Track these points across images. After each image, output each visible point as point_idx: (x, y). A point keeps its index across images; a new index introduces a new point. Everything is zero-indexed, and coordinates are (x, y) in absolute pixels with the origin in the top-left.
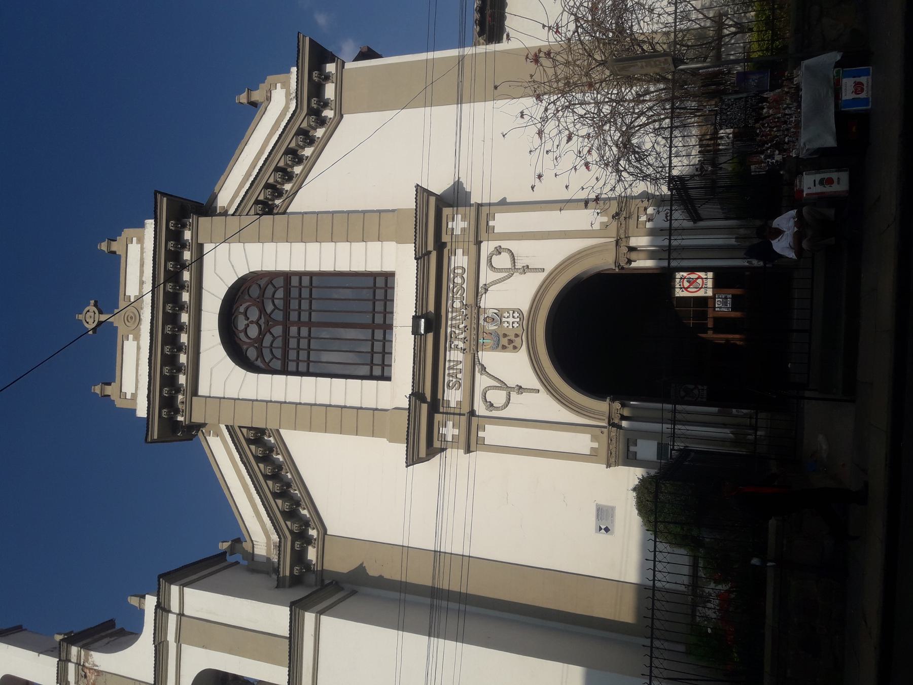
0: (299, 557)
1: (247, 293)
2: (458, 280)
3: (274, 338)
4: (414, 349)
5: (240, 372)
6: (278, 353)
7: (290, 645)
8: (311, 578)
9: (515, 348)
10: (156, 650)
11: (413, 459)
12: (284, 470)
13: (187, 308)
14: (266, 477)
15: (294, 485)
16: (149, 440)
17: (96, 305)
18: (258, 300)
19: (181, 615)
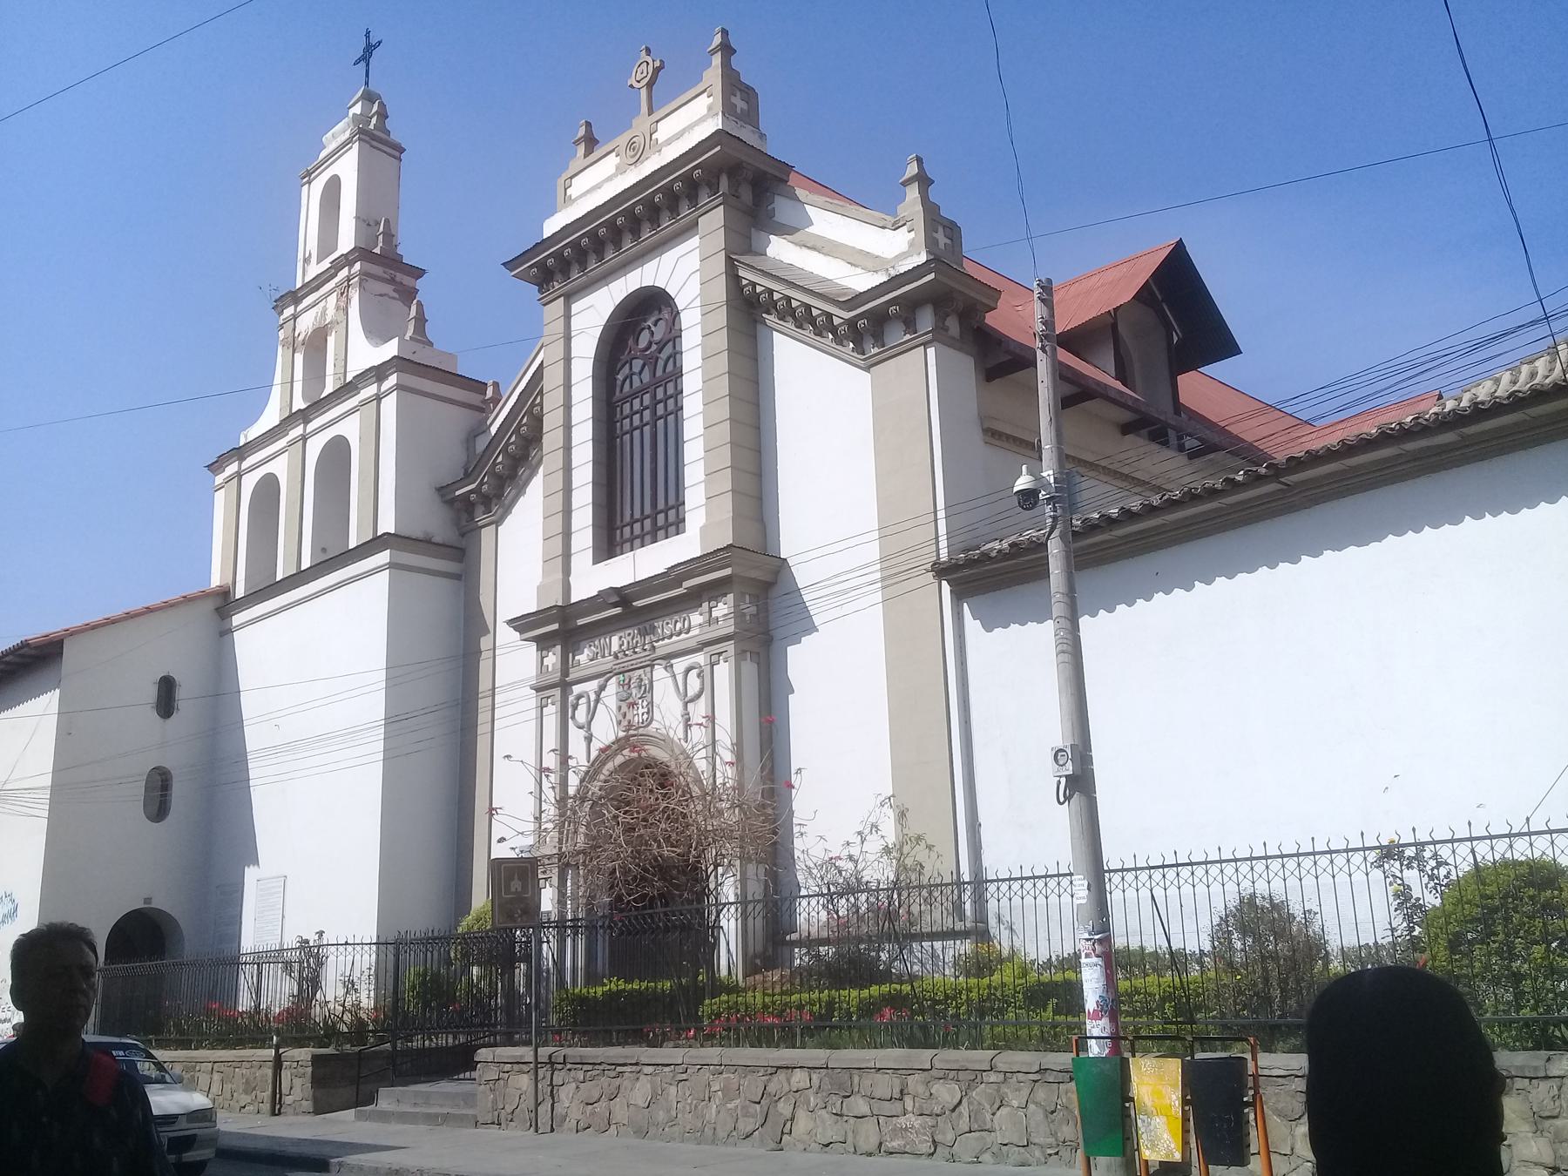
2: (679, 625)
8: (465, 516)
9: (619, 723)
11: (522, 624)
17: (657, 71)
18: (673, 331)
19: (378, 398)
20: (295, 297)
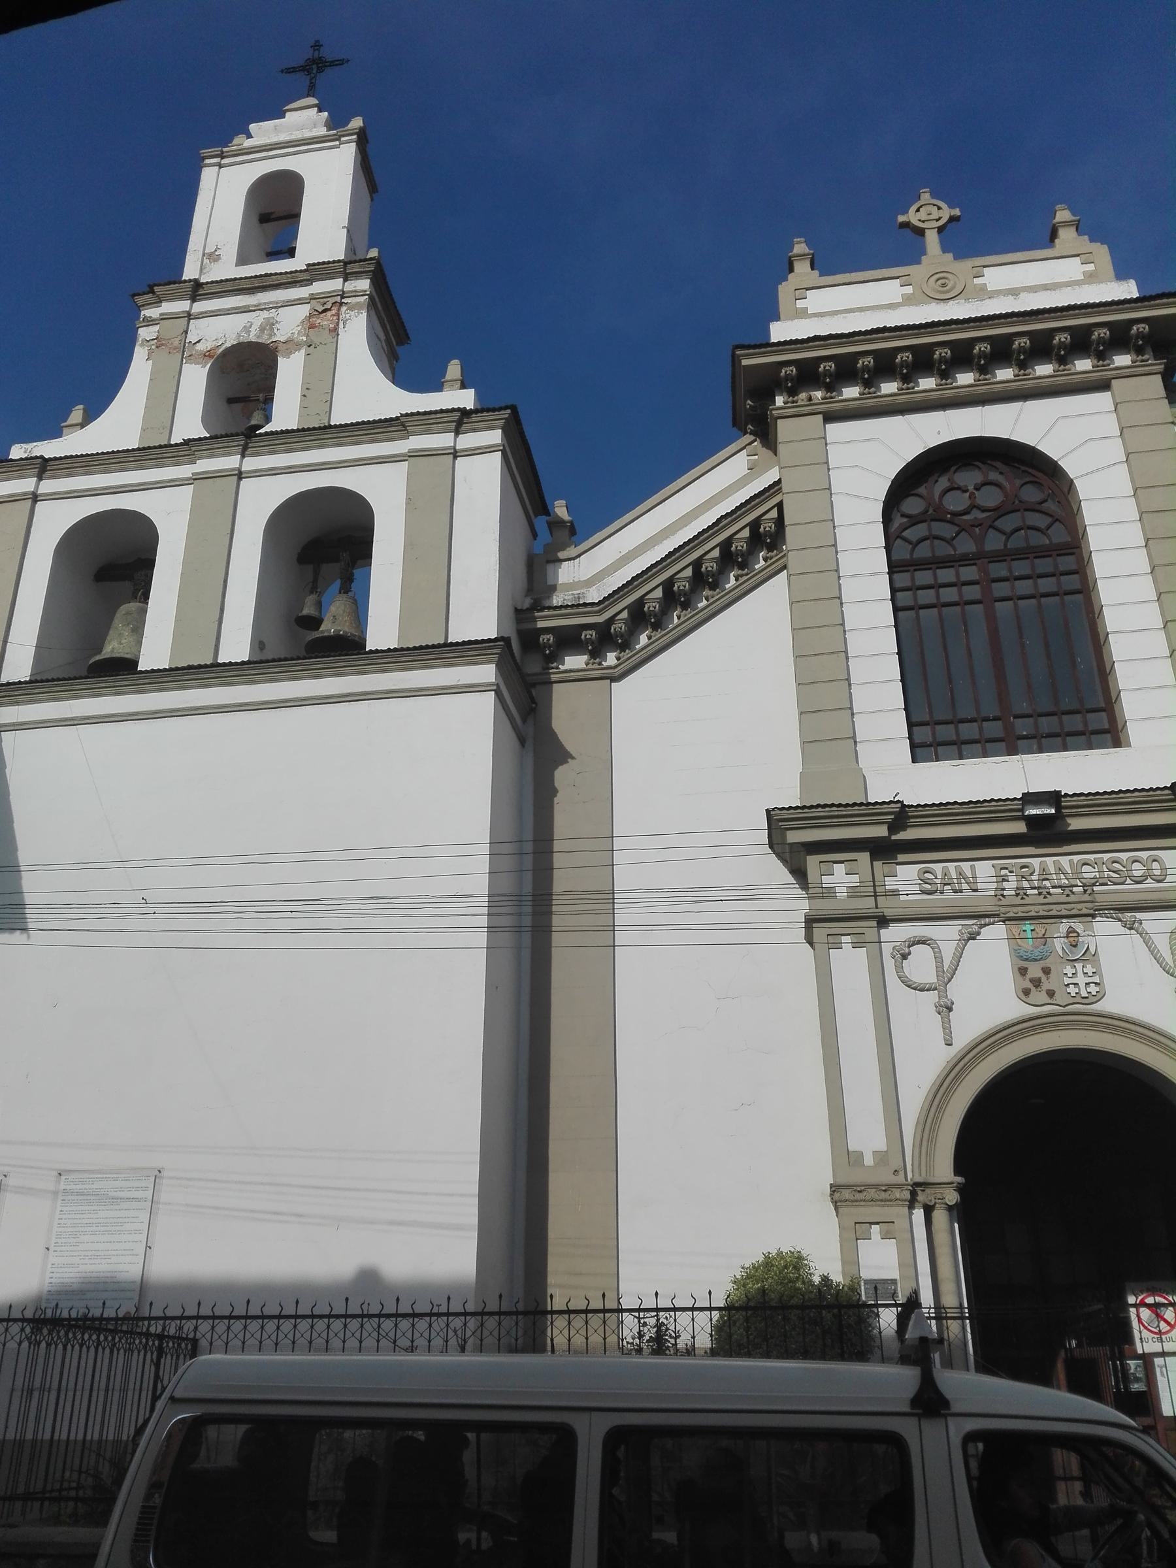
0: (569, 640)
1: (1022, 482)
2: (1138, 870)
3: (949, 541)
4: (992, 800)
5: (881, 490)
6: (923, 551)
7: (433, 646)
9: (1027, 992)
10: (391, 419)
12: (711, 593)
13: (986, 380)
14: (697, 564)
15: (688, 613)
16: (739, 352)
17: (952, 219)
18: (1017, 502)
19: (455, 454)
20: (197, 290)
